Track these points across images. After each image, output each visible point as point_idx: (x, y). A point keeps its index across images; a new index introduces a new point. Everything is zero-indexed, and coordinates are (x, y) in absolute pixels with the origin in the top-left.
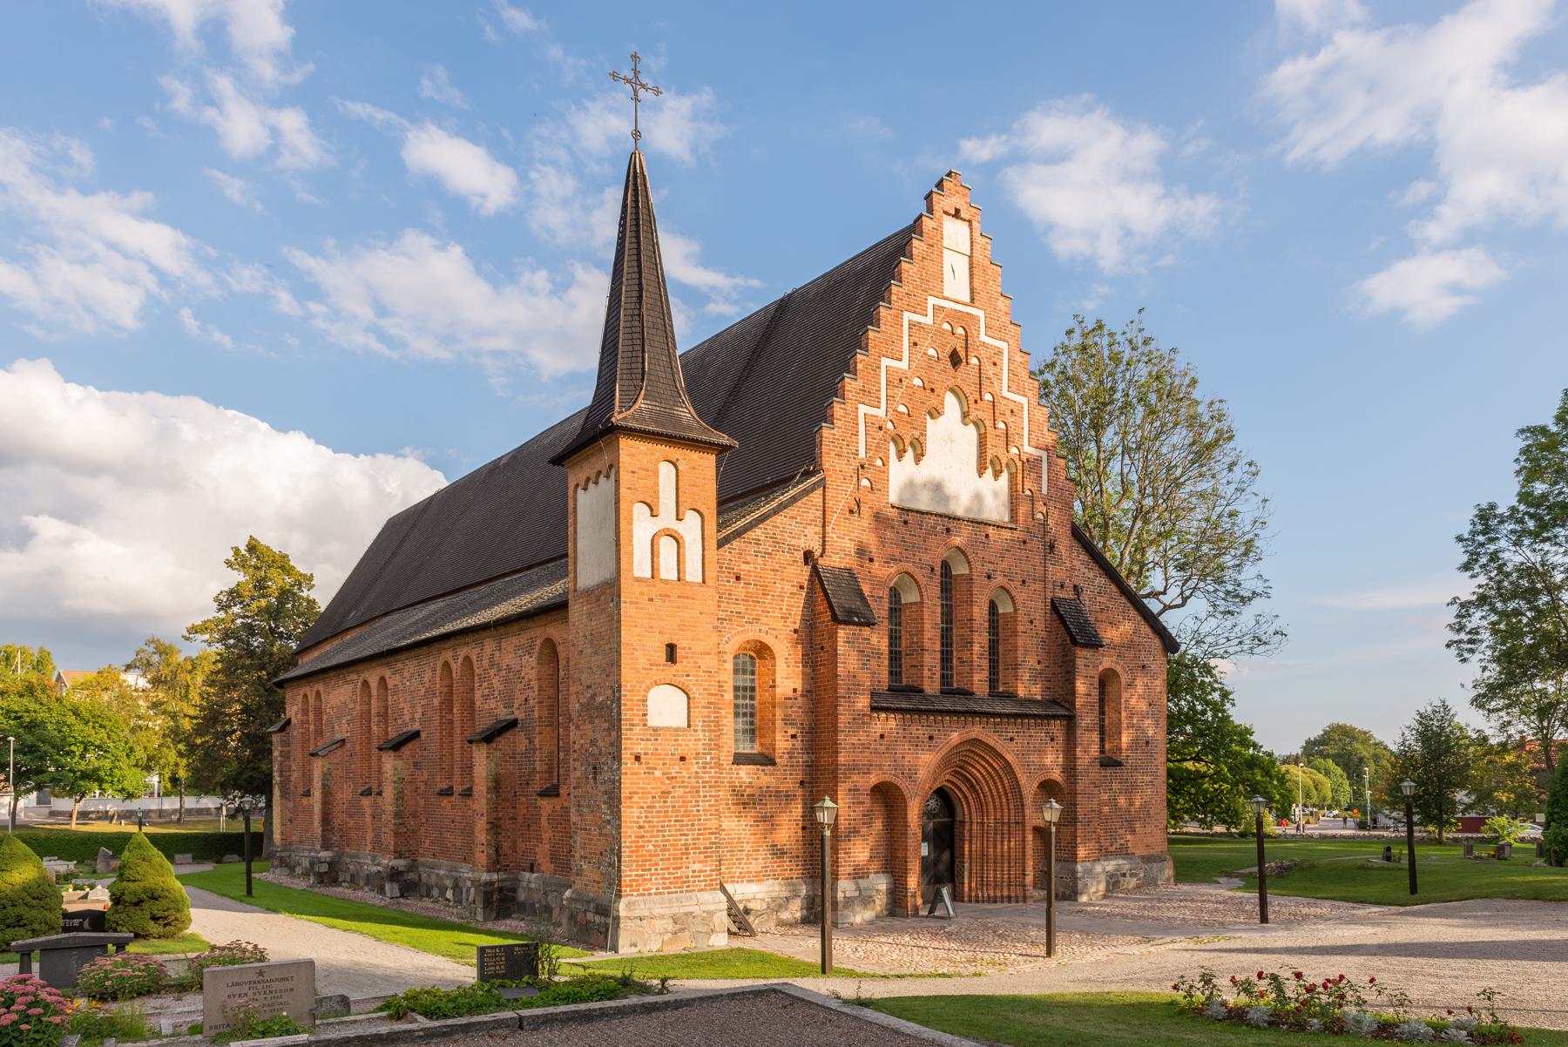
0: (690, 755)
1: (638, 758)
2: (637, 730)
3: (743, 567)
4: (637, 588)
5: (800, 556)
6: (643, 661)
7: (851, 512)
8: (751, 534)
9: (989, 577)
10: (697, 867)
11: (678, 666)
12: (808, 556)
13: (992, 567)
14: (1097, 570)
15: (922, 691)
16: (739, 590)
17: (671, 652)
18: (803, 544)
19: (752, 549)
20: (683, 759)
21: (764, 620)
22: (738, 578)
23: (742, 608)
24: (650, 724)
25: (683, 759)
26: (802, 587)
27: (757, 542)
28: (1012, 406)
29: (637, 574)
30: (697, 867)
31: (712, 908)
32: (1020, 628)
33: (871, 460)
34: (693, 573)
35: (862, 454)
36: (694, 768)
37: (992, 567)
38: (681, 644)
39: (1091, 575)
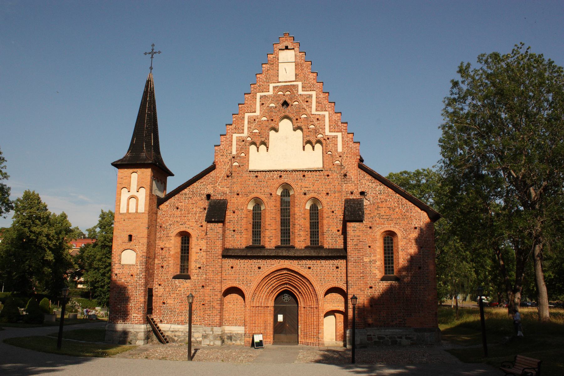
0: (134, 274)
1: (116, 275)
2: (117, 265)
3: (179, 204)
4: (120, 216)
5: (204, 197)
6: (120, 241)
7: (228, 176)
8: (183, 192)
9: (305, 194)
10: (135, 315)
11: (132, 242)
12: (208, 196)
13: (307, 189)
14: (378, 183)
15: (265, 248)
16: (178, 212)
17: (130, 237)
18: (206, 192)
19: (183, 197)
20: (132, 275)
21: (187, 223)
22: (178, 208)
23: (179, 219)
24: (122, 263)
25: (132, 275)
26: (205, 209)
27: (185, 194)
28: (318, 117)
29: (121, 212)
30: (135, 315)
31: (138, 330)
32: (325, 215)
33: (238, 155)
34: (142, 208)
35: (234, 152)
36: (136, 279)
37: (307, 189)
38: (134, 235)
39: (374, 185)
